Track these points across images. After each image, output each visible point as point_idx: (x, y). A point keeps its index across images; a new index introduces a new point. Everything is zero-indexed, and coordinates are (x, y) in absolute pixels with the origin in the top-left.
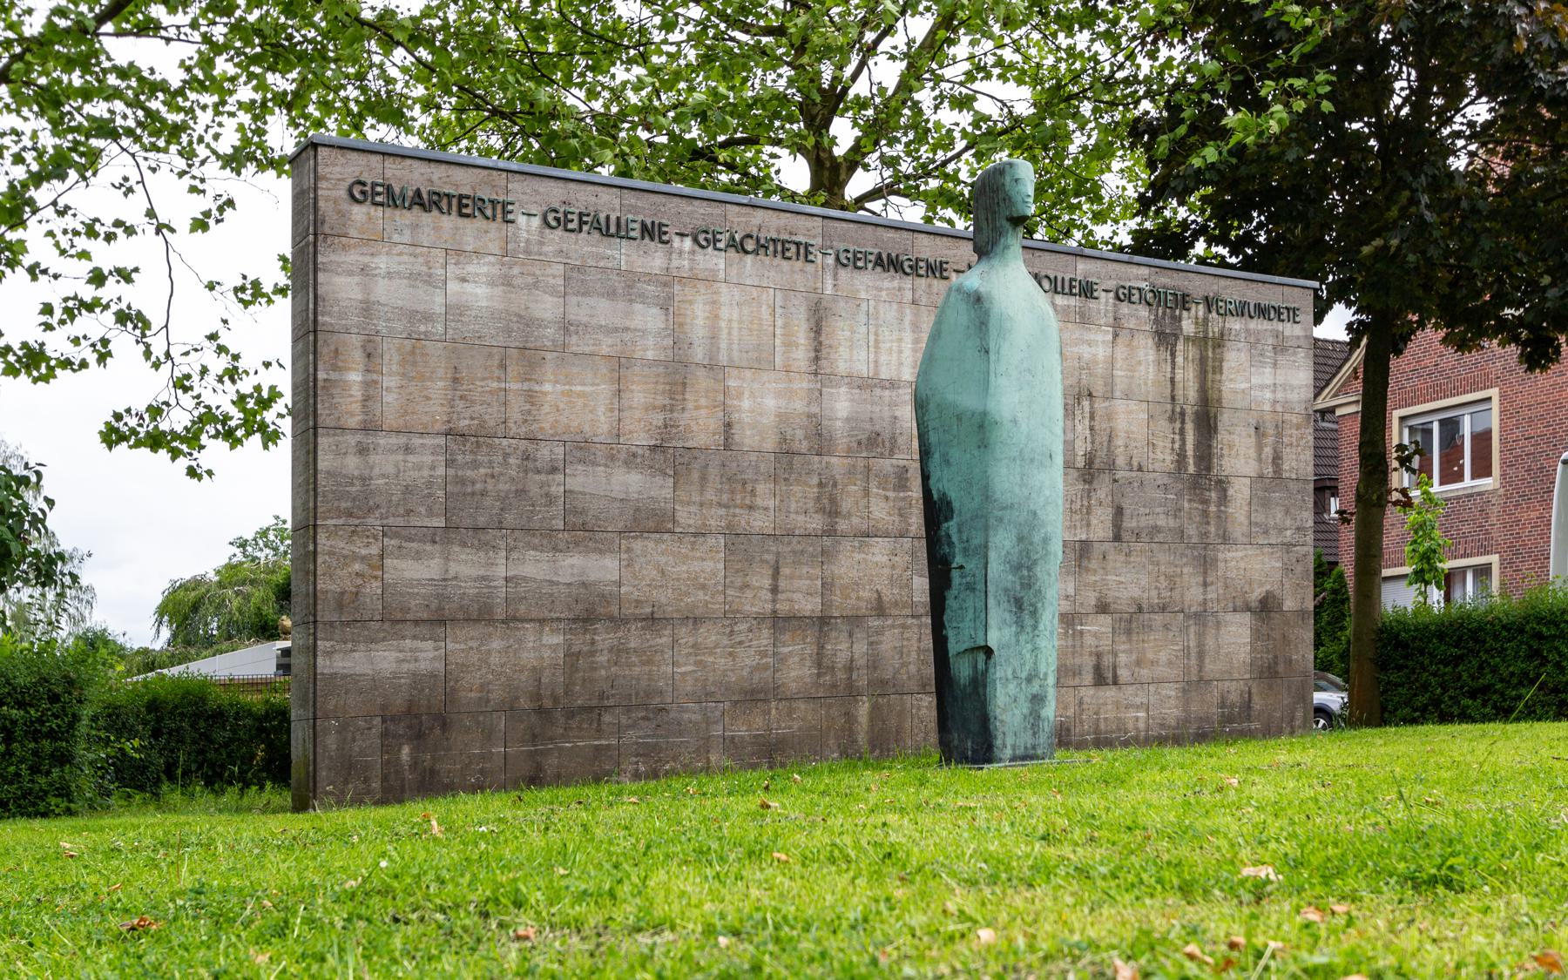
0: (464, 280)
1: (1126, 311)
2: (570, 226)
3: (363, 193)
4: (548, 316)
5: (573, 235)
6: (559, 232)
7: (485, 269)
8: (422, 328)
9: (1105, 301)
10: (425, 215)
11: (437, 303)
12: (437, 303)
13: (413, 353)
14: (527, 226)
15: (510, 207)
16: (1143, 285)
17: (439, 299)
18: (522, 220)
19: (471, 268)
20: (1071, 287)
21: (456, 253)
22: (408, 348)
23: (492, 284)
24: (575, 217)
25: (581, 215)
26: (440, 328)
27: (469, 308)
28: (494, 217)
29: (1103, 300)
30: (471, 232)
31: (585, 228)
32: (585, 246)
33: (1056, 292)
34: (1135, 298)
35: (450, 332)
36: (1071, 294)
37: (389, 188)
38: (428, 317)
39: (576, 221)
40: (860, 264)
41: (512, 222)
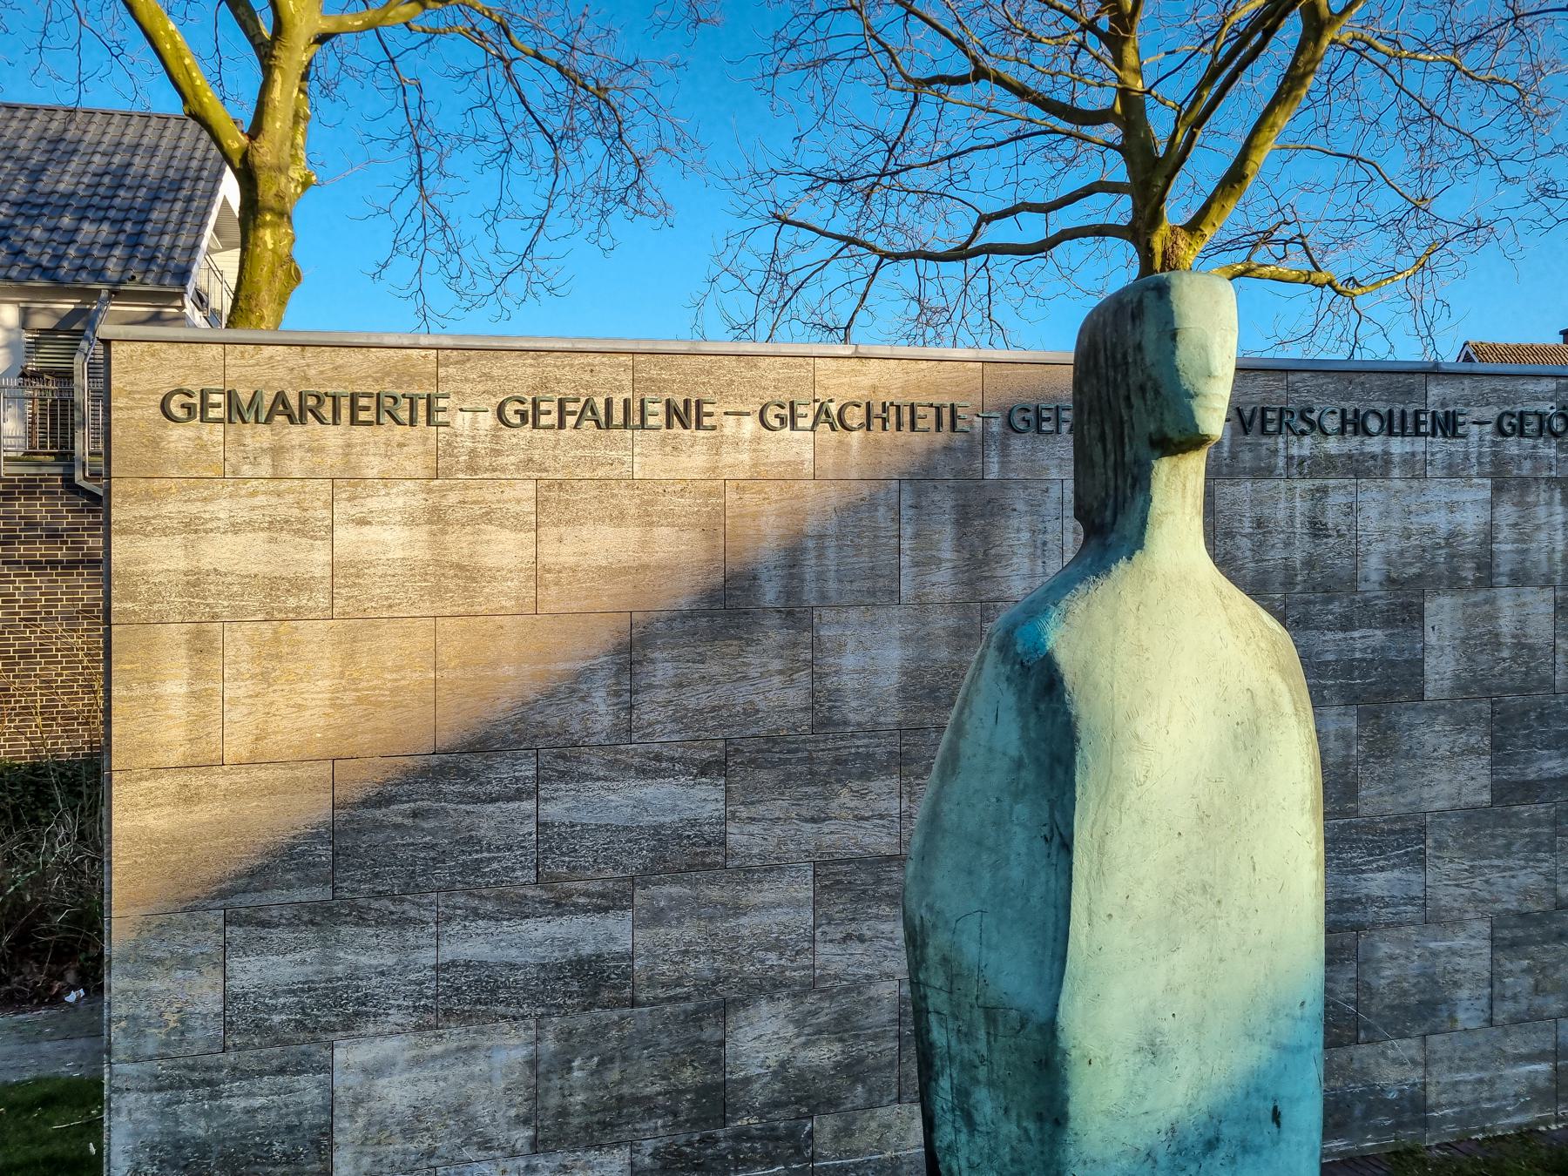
0: (363, 522)
1: (1514, 450)
2: (544, 420)
3: (189, 408)
4: (508, 561)
5: (549, 434)
6: (527, 431)
7: (400, 502)
8: (292, 602)
9: (1477, 437)
10: (296, 429)
11: (316, 559)
12: (316, 559)
13: (277, 639)
14: (470, 423)
15: (442, 403)
16: (1547, 407)
17: (321, 556)
18: (462, 421)
19: (373, 503)
20: (1417, 423)
21: (348, 480)
22: (269, 635)
23: (411, 522)
24: (554, 407)
25: (561, 403)
26: (324, 601)
27: (371, 564)
28: (412, 422)
29: (1474, 439)
30: (373, 447)
31: (571, 420)
32: (569, 447)
33: (1391, 433)
34: (1532, 425)
35: (339, 602)
36: (1417, 433)
37: (231, 396)
38: (299, 585)
39: (555, 415)
40: (1046, 426)
41: (447, 425)
